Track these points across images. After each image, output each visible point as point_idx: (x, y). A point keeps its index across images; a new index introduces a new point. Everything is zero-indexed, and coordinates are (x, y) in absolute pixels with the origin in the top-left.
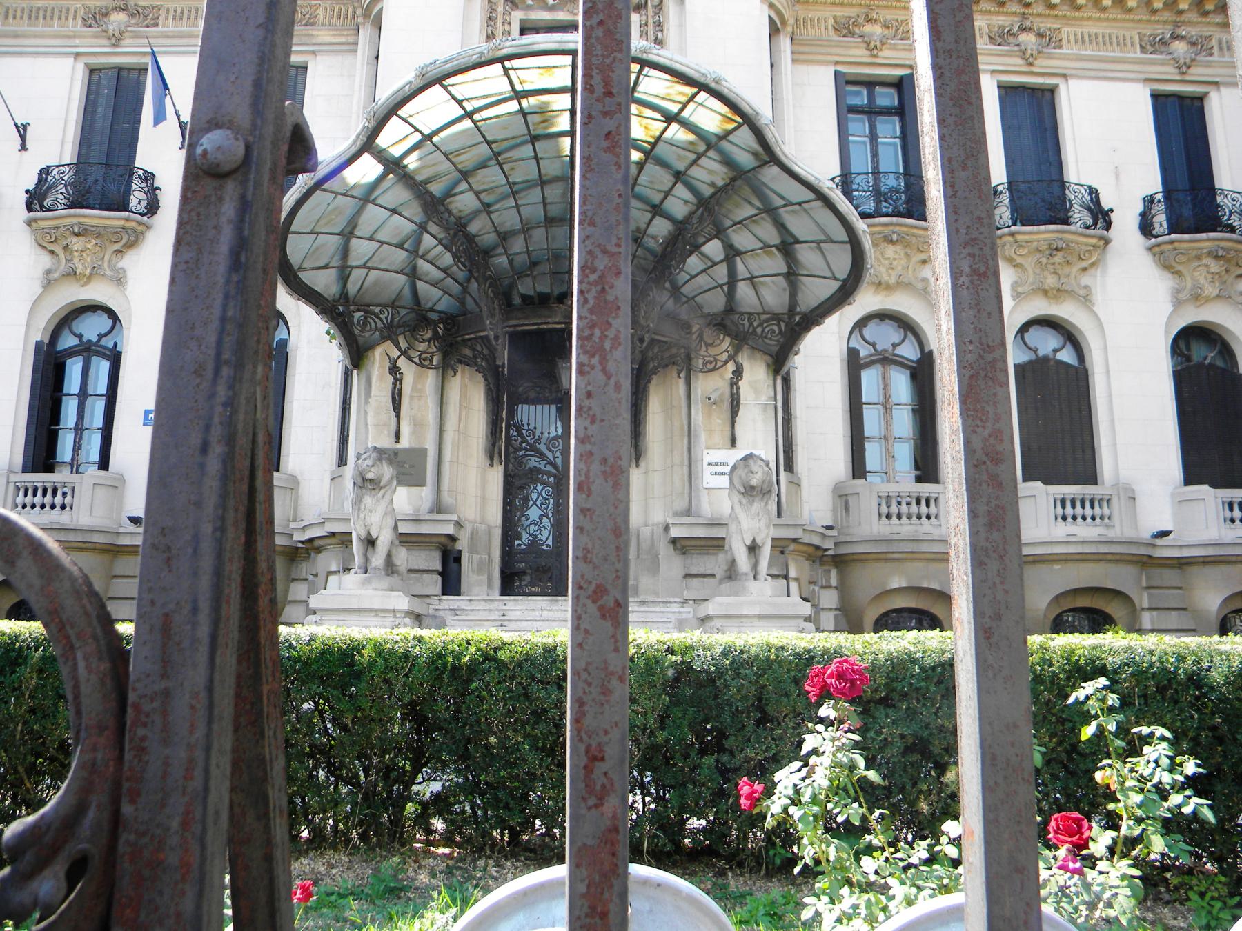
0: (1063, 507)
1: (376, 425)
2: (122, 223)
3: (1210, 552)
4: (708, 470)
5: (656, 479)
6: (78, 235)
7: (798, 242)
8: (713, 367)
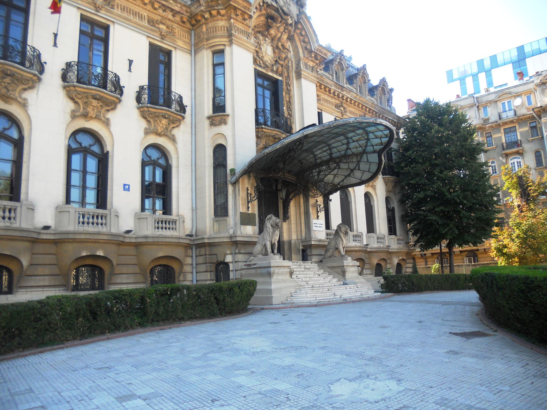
0: (158, 223)
1: (242, 204)
2: (115, 99)
3: (377, 250)
4: (314, 225)
5: (293, 226)
6: (95, 99)
7: (359, 169)
8: (314, 197)
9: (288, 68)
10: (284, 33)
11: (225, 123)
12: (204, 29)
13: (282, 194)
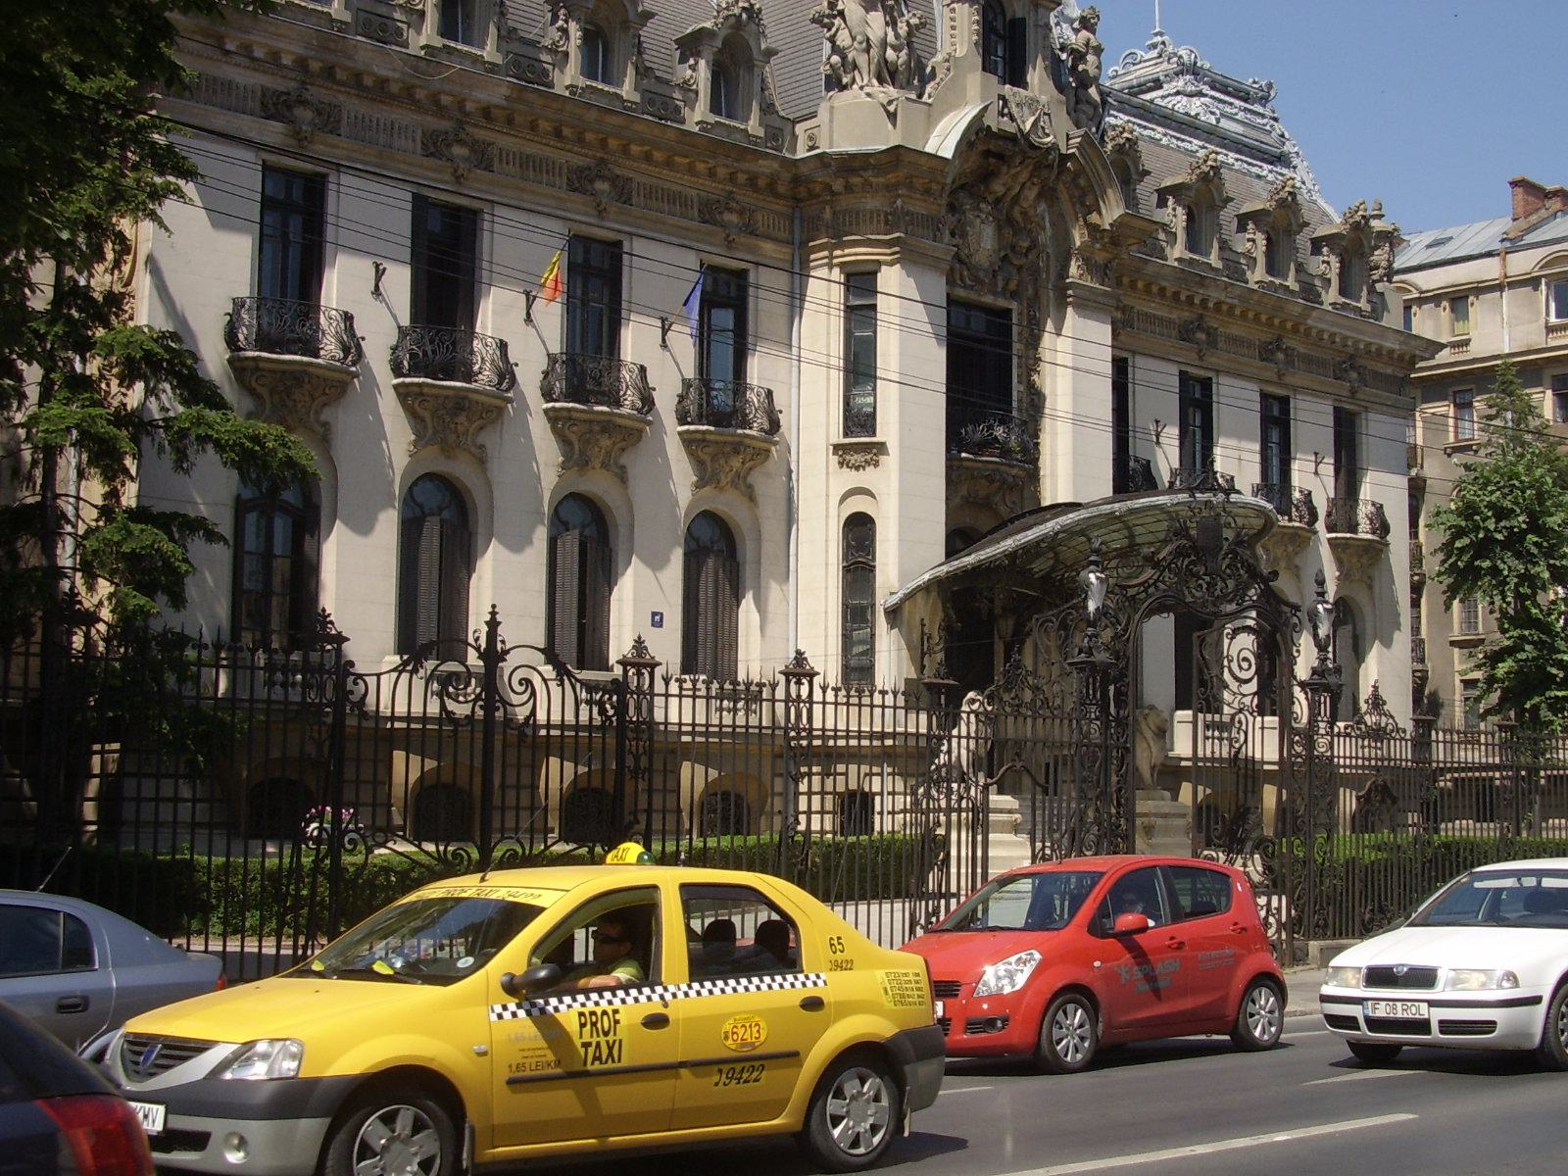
9: (1035, 272)
10: (1028, 184)
11: (876, 464)
12: (828, 214)
13: (1007, 626)
